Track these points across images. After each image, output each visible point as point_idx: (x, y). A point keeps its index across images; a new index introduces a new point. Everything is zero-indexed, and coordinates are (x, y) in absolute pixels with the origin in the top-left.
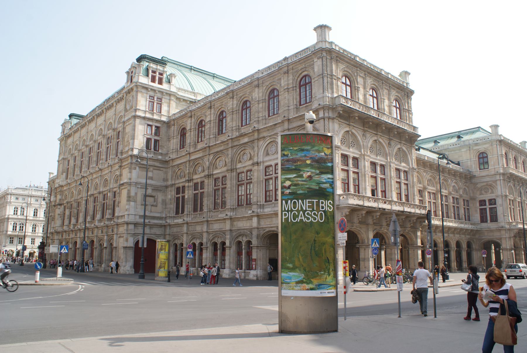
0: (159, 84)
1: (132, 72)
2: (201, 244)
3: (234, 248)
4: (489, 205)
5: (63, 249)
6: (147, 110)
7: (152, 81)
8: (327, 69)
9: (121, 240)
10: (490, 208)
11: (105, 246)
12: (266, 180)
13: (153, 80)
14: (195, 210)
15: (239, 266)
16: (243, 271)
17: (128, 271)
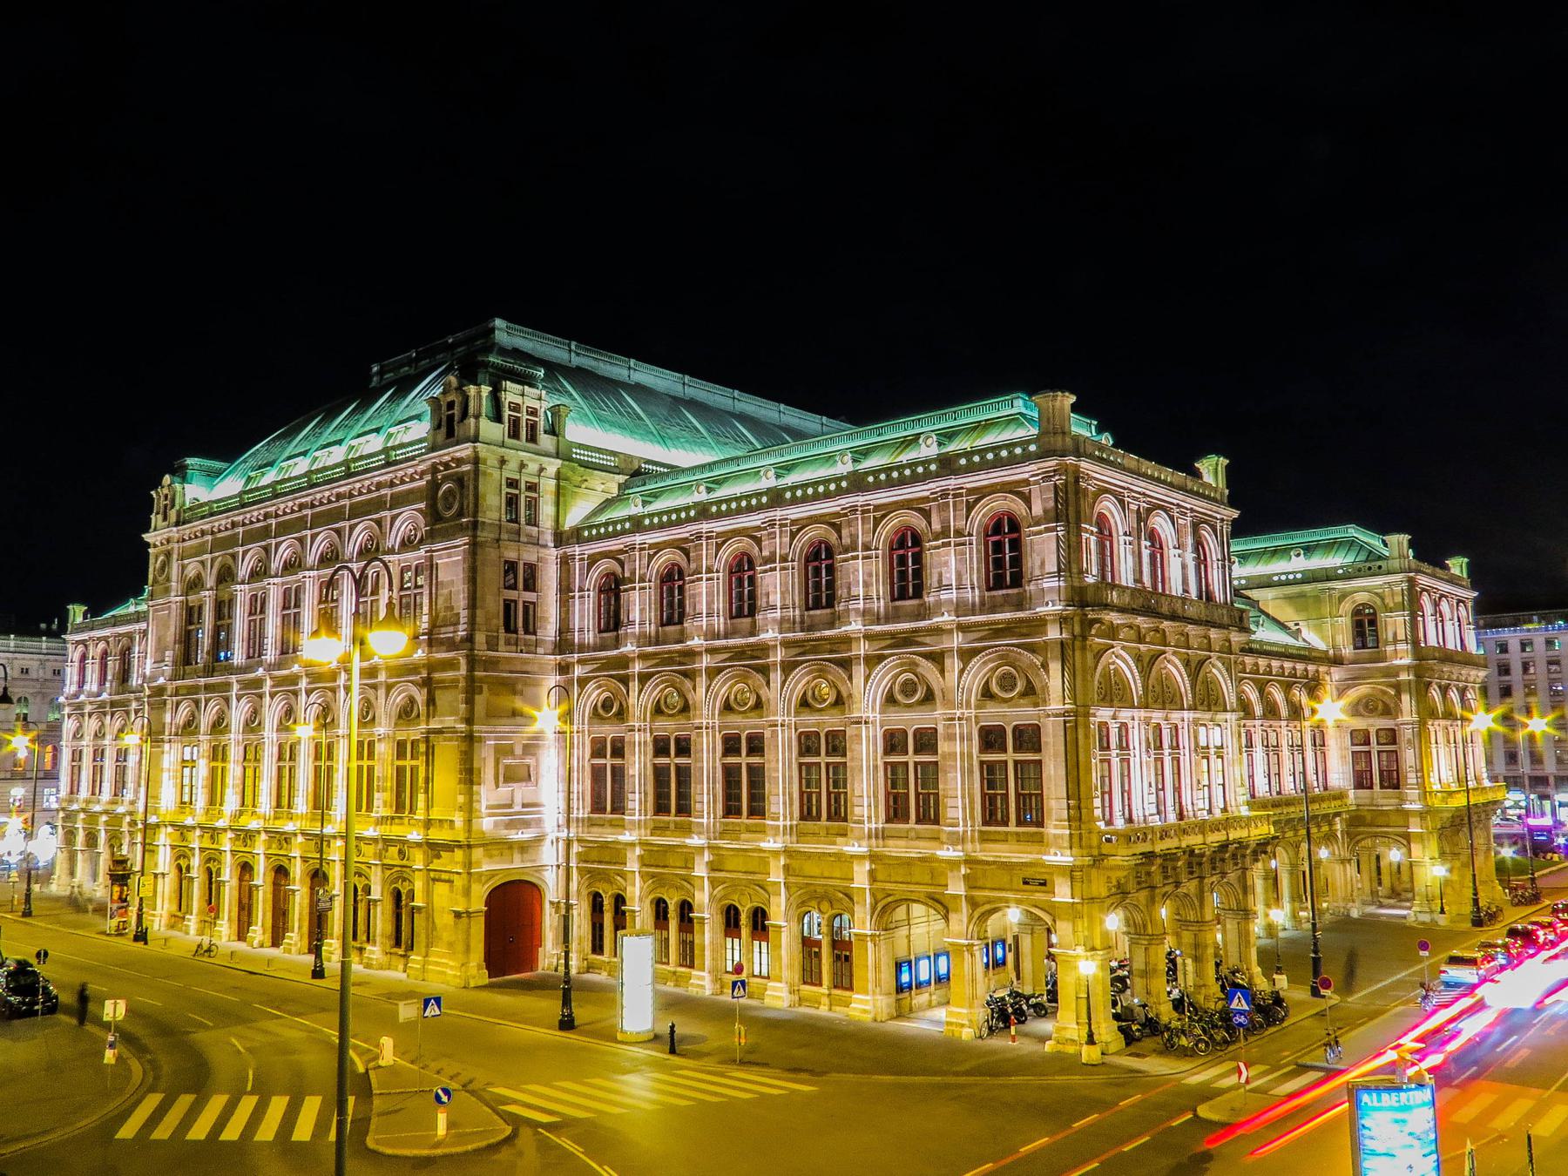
0: (527, 440)
1: (451, 405)
2: (686, 907)
3: (795, 927)
4: (1378, 744)
5: (428, 1010)
6: (503, 516)
7: (509, 437)
8: (1067, 510)
9: (441, 889)
10: (1379, 752)
11: (376, 894)
12: (886, 764)
13: (514, 434)
14: (661, 808)
15: (810, 975)
16: (824, 990)
17: (474, 978)
